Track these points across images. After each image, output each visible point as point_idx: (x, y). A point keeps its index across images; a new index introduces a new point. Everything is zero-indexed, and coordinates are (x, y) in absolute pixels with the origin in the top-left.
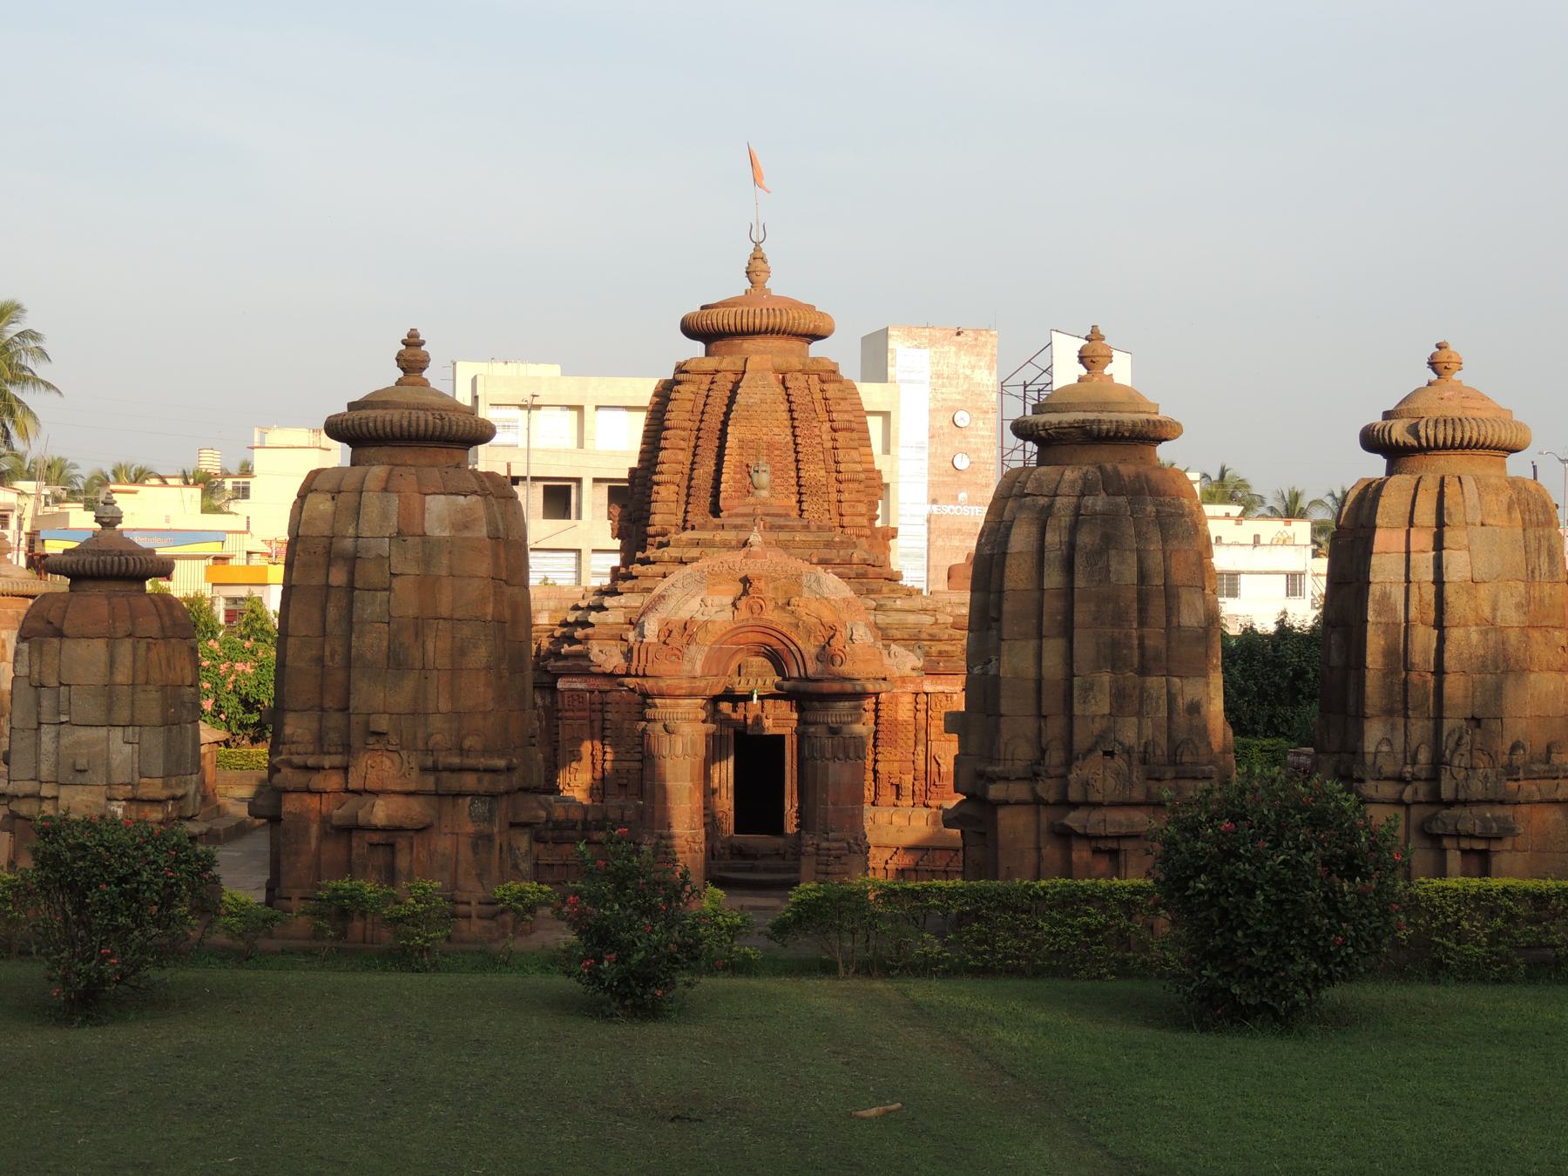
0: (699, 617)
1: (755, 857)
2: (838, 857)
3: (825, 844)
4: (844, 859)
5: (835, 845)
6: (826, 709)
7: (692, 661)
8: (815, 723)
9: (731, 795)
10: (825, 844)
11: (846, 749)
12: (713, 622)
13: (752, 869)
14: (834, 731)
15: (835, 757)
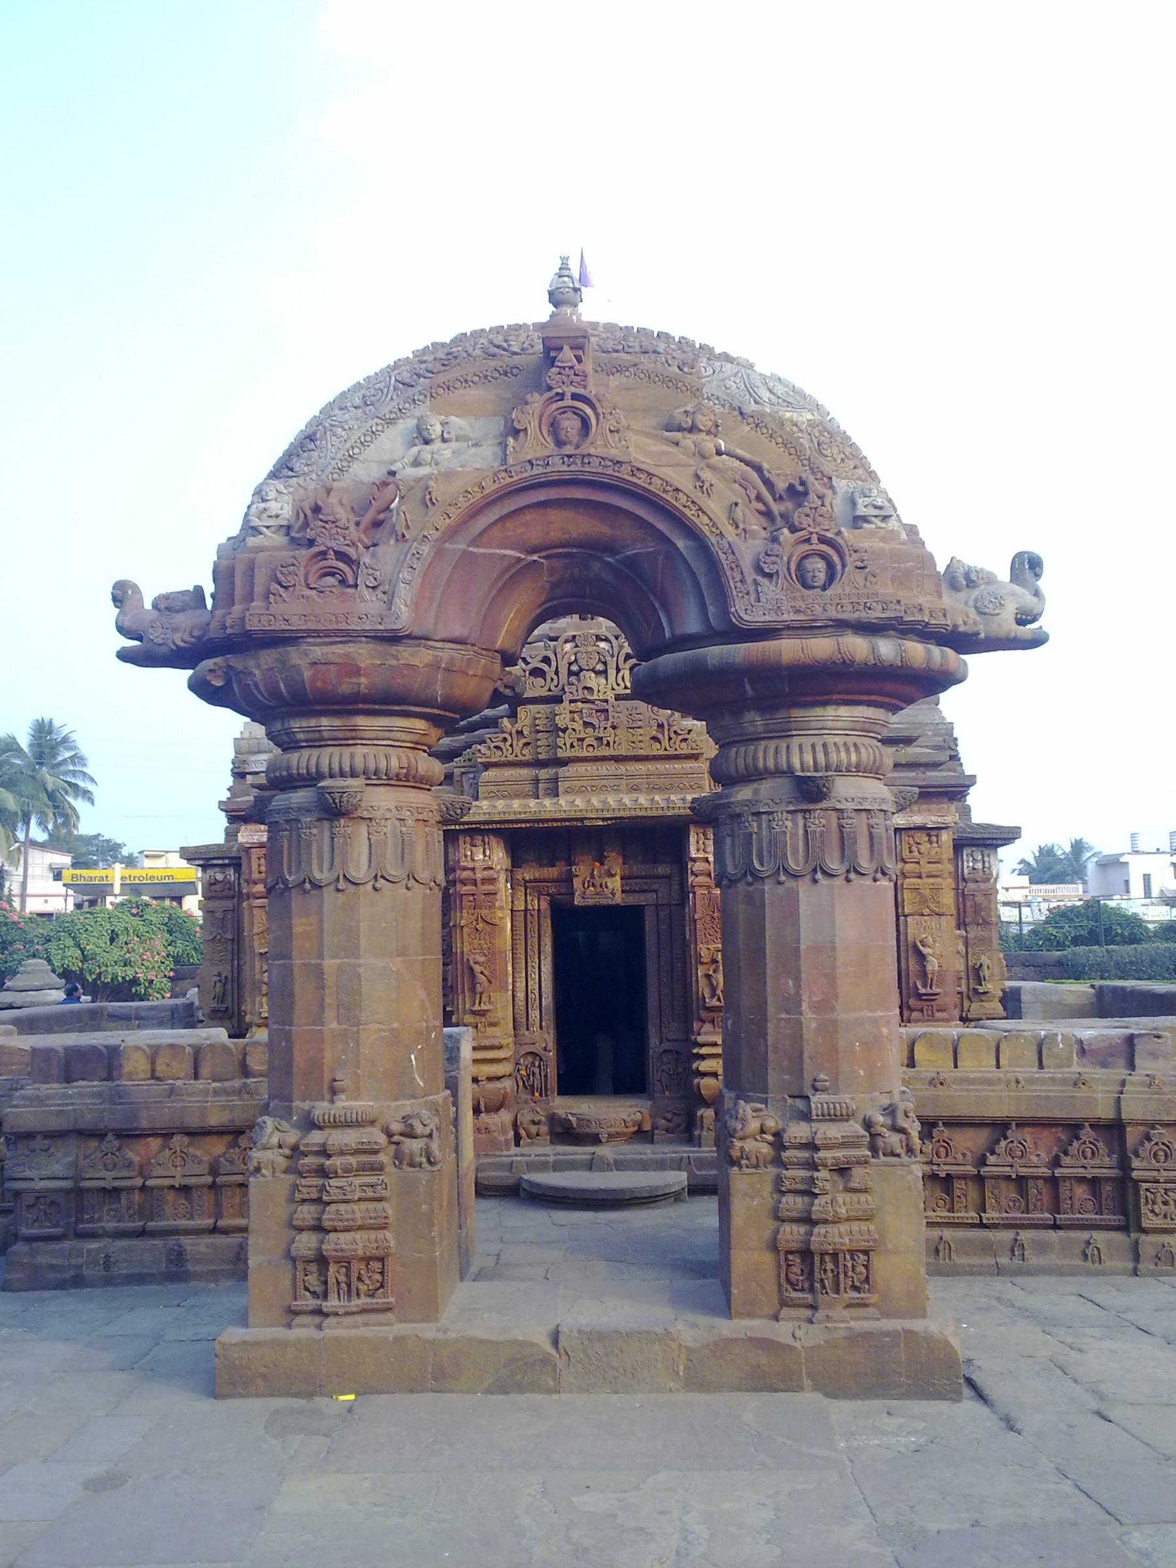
0: (408, 473)
1: (595, 1140)
2: (842, 1171)
3: (798, 1131)
4: (858, 1176)
5: (832, 1131)
6: (783, 732)
7: (385, 590)
8: (753, 776)
9: (549, 1022)
10: (798, 1131)
11: (845, 843)
12: (449, 475)
13: (590, 1165)
14: (810, 791)
15: (819, 870)
